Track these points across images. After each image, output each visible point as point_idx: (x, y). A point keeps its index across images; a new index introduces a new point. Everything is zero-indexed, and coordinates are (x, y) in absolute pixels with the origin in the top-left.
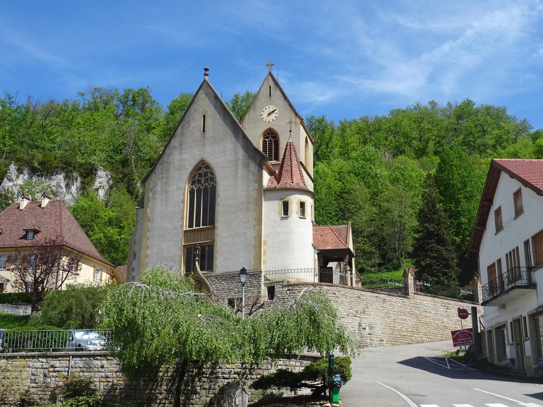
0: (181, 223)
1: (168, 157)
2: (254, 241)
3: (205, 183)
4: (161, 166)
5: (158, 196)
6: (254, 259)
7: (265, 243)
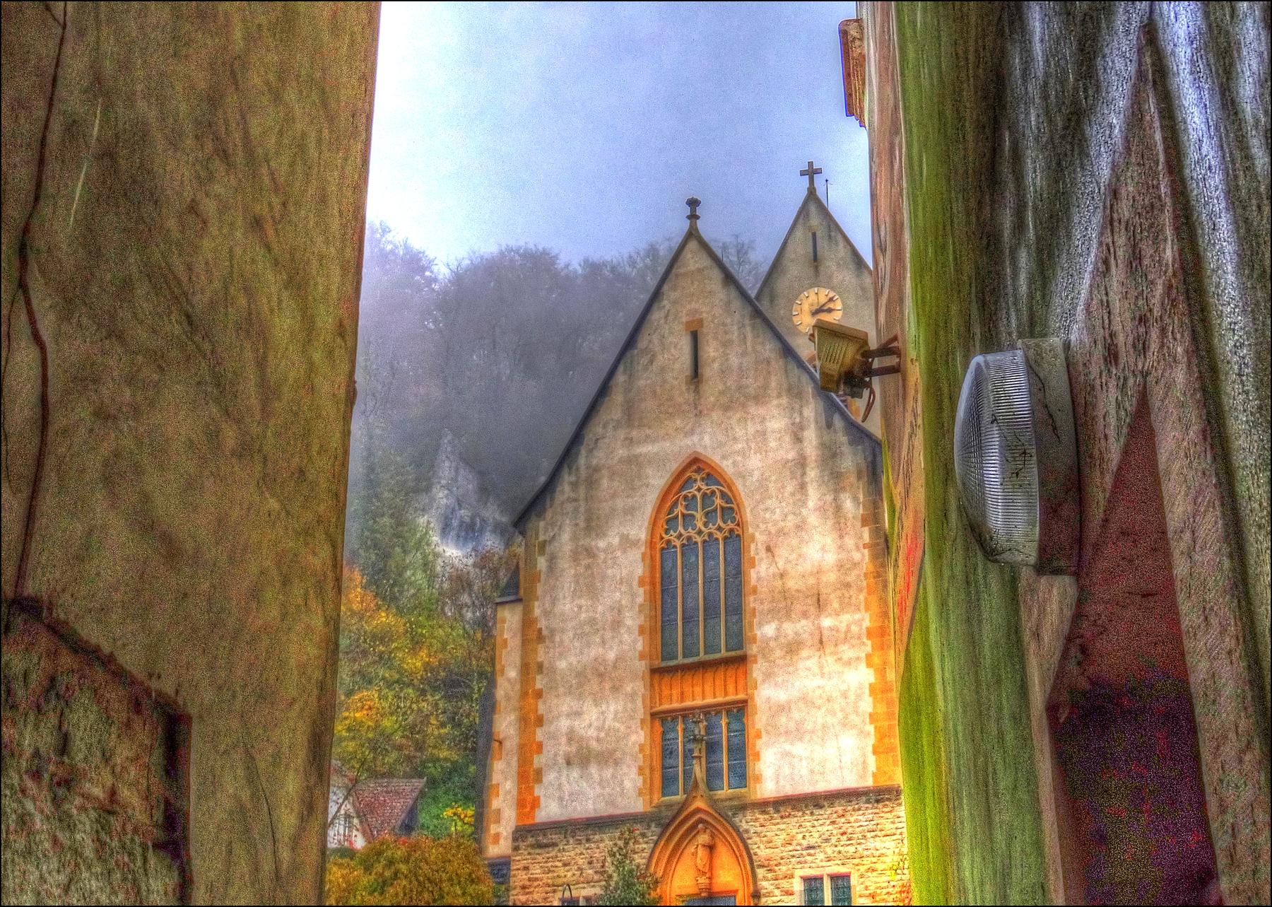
1: (591, 451)
3: (706, 524)
5: (564, 564)
6: (875, 752)
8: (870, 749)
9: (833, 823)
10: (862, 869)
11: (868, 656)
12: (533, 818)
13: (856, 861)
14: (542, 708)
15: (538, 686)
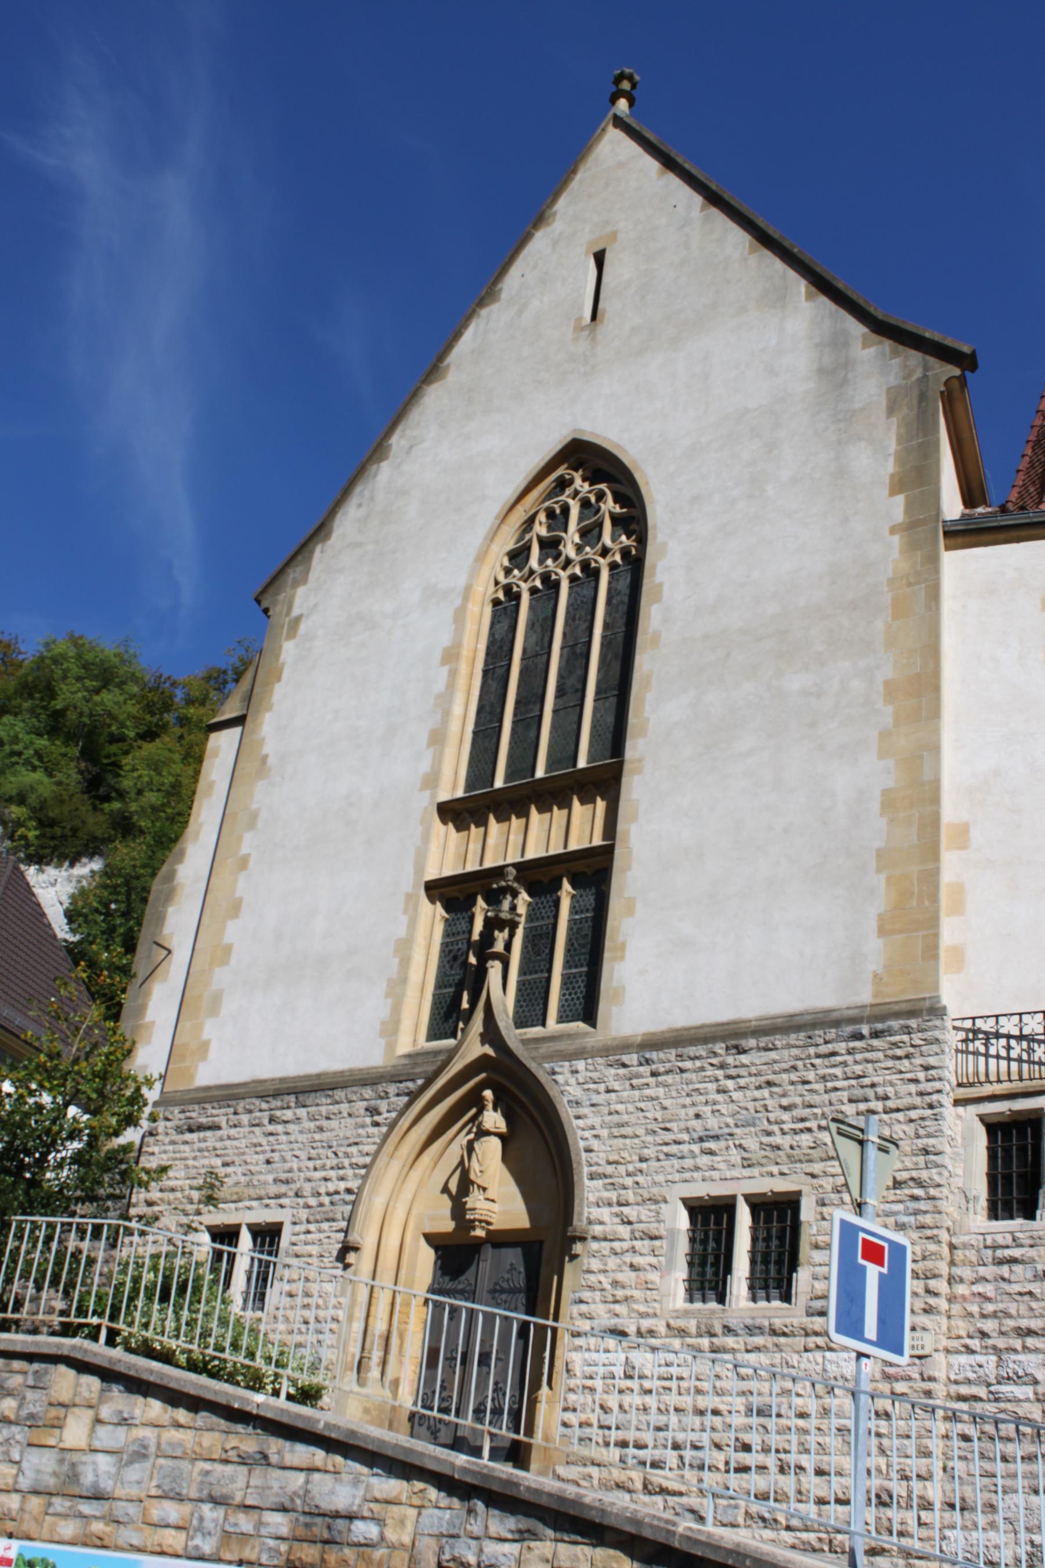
0: (425, 766)
2: (882, 823)
4: (361, 513)
6: (882, 932)
7: (962, 835)
8: (873, 924)
9: (769, 1084)
10: (827, 1183)
11: (884, 735)
12: (192, 1077)
13: (817, 1168)
14: (242, 887)
15: (244, 850)
